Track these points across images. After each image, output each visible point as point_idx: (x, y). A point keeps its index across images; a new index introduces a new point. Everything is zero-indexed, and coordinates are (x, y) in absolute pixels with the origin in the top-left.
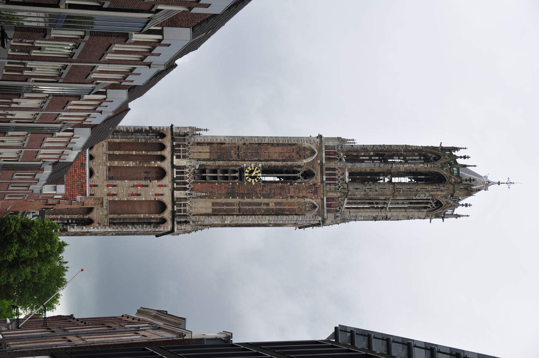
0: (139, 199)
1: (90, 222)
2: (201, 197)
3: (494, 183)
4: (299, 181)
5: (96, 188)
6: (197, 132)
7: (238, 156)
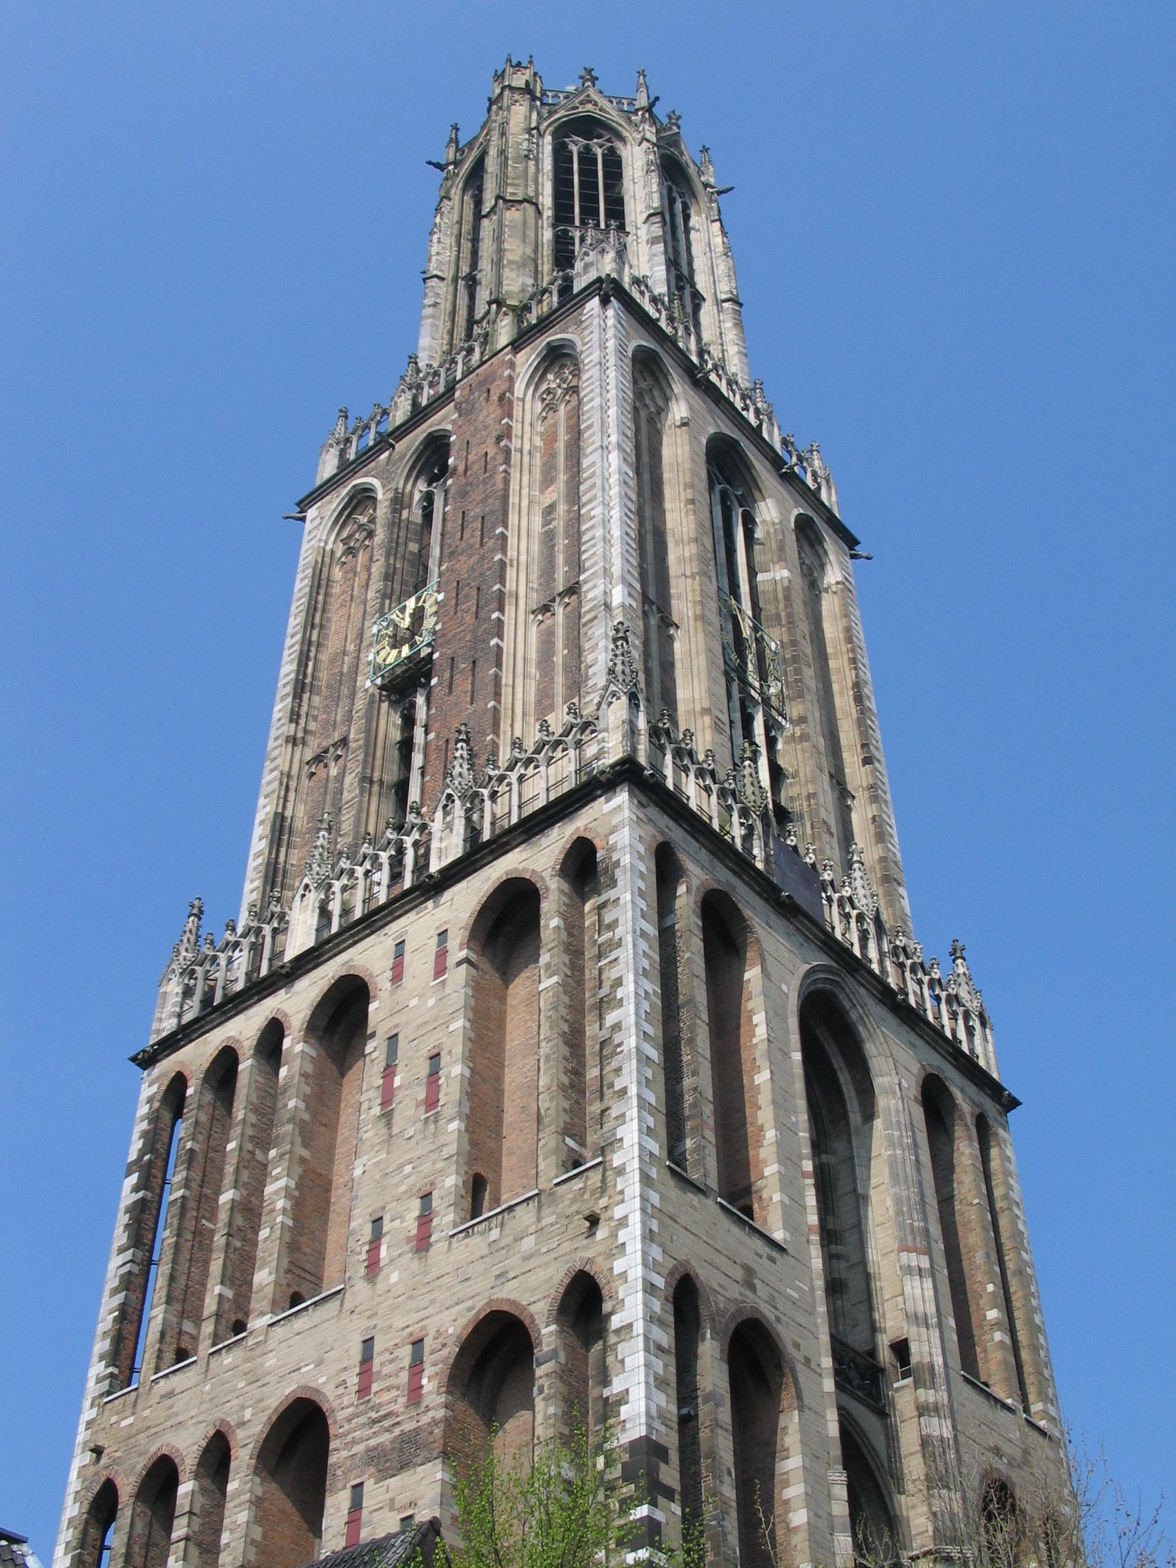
0: (458, 1050)
1: (584, 1301)
5: (378, 1346)
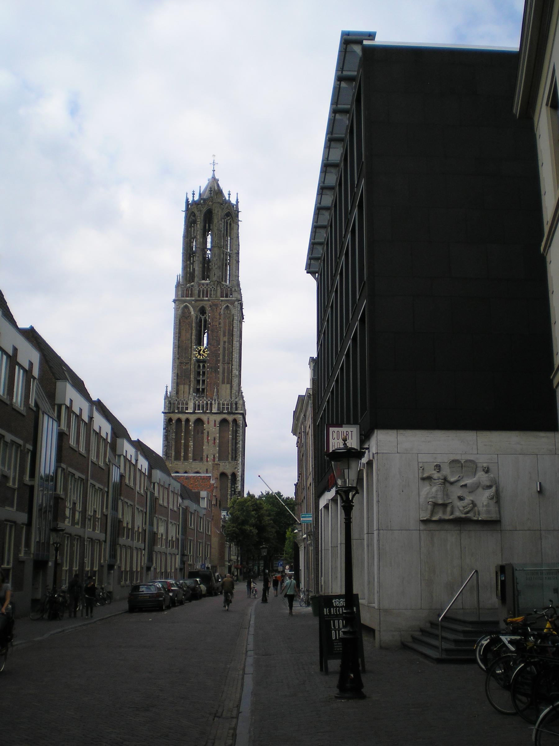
1: (234, 475)
2: (218, 392)
3: (214, 174)
4: (207, 318)
6: (169, 393)
7: (187, 363)
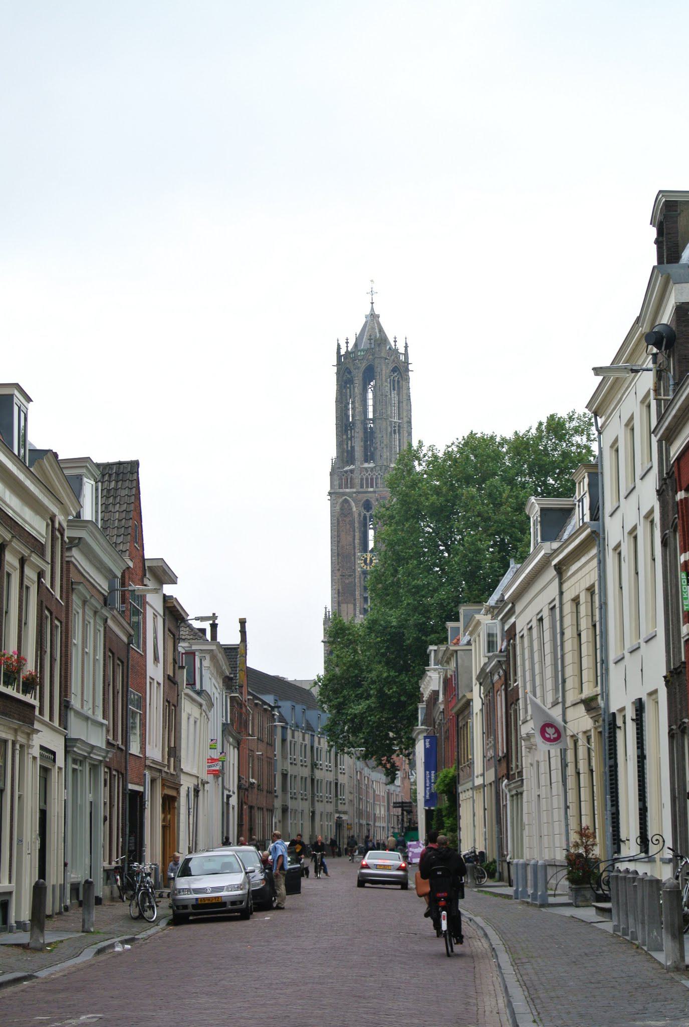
3: (372, 309)
7: (350, 576)
